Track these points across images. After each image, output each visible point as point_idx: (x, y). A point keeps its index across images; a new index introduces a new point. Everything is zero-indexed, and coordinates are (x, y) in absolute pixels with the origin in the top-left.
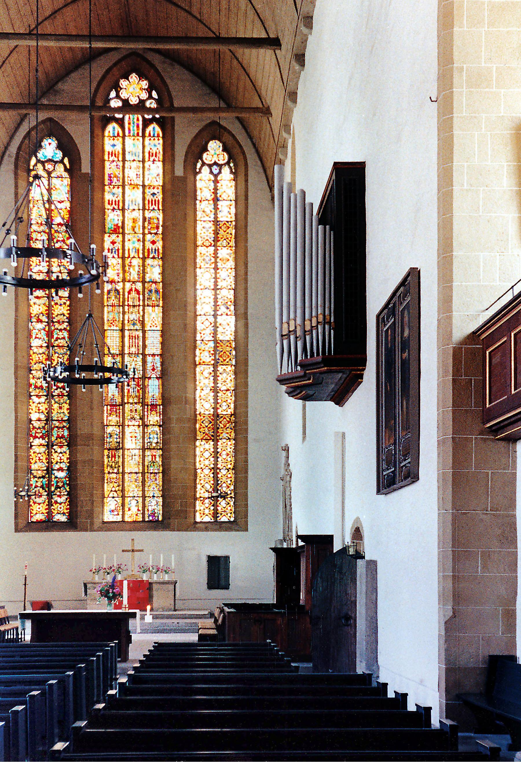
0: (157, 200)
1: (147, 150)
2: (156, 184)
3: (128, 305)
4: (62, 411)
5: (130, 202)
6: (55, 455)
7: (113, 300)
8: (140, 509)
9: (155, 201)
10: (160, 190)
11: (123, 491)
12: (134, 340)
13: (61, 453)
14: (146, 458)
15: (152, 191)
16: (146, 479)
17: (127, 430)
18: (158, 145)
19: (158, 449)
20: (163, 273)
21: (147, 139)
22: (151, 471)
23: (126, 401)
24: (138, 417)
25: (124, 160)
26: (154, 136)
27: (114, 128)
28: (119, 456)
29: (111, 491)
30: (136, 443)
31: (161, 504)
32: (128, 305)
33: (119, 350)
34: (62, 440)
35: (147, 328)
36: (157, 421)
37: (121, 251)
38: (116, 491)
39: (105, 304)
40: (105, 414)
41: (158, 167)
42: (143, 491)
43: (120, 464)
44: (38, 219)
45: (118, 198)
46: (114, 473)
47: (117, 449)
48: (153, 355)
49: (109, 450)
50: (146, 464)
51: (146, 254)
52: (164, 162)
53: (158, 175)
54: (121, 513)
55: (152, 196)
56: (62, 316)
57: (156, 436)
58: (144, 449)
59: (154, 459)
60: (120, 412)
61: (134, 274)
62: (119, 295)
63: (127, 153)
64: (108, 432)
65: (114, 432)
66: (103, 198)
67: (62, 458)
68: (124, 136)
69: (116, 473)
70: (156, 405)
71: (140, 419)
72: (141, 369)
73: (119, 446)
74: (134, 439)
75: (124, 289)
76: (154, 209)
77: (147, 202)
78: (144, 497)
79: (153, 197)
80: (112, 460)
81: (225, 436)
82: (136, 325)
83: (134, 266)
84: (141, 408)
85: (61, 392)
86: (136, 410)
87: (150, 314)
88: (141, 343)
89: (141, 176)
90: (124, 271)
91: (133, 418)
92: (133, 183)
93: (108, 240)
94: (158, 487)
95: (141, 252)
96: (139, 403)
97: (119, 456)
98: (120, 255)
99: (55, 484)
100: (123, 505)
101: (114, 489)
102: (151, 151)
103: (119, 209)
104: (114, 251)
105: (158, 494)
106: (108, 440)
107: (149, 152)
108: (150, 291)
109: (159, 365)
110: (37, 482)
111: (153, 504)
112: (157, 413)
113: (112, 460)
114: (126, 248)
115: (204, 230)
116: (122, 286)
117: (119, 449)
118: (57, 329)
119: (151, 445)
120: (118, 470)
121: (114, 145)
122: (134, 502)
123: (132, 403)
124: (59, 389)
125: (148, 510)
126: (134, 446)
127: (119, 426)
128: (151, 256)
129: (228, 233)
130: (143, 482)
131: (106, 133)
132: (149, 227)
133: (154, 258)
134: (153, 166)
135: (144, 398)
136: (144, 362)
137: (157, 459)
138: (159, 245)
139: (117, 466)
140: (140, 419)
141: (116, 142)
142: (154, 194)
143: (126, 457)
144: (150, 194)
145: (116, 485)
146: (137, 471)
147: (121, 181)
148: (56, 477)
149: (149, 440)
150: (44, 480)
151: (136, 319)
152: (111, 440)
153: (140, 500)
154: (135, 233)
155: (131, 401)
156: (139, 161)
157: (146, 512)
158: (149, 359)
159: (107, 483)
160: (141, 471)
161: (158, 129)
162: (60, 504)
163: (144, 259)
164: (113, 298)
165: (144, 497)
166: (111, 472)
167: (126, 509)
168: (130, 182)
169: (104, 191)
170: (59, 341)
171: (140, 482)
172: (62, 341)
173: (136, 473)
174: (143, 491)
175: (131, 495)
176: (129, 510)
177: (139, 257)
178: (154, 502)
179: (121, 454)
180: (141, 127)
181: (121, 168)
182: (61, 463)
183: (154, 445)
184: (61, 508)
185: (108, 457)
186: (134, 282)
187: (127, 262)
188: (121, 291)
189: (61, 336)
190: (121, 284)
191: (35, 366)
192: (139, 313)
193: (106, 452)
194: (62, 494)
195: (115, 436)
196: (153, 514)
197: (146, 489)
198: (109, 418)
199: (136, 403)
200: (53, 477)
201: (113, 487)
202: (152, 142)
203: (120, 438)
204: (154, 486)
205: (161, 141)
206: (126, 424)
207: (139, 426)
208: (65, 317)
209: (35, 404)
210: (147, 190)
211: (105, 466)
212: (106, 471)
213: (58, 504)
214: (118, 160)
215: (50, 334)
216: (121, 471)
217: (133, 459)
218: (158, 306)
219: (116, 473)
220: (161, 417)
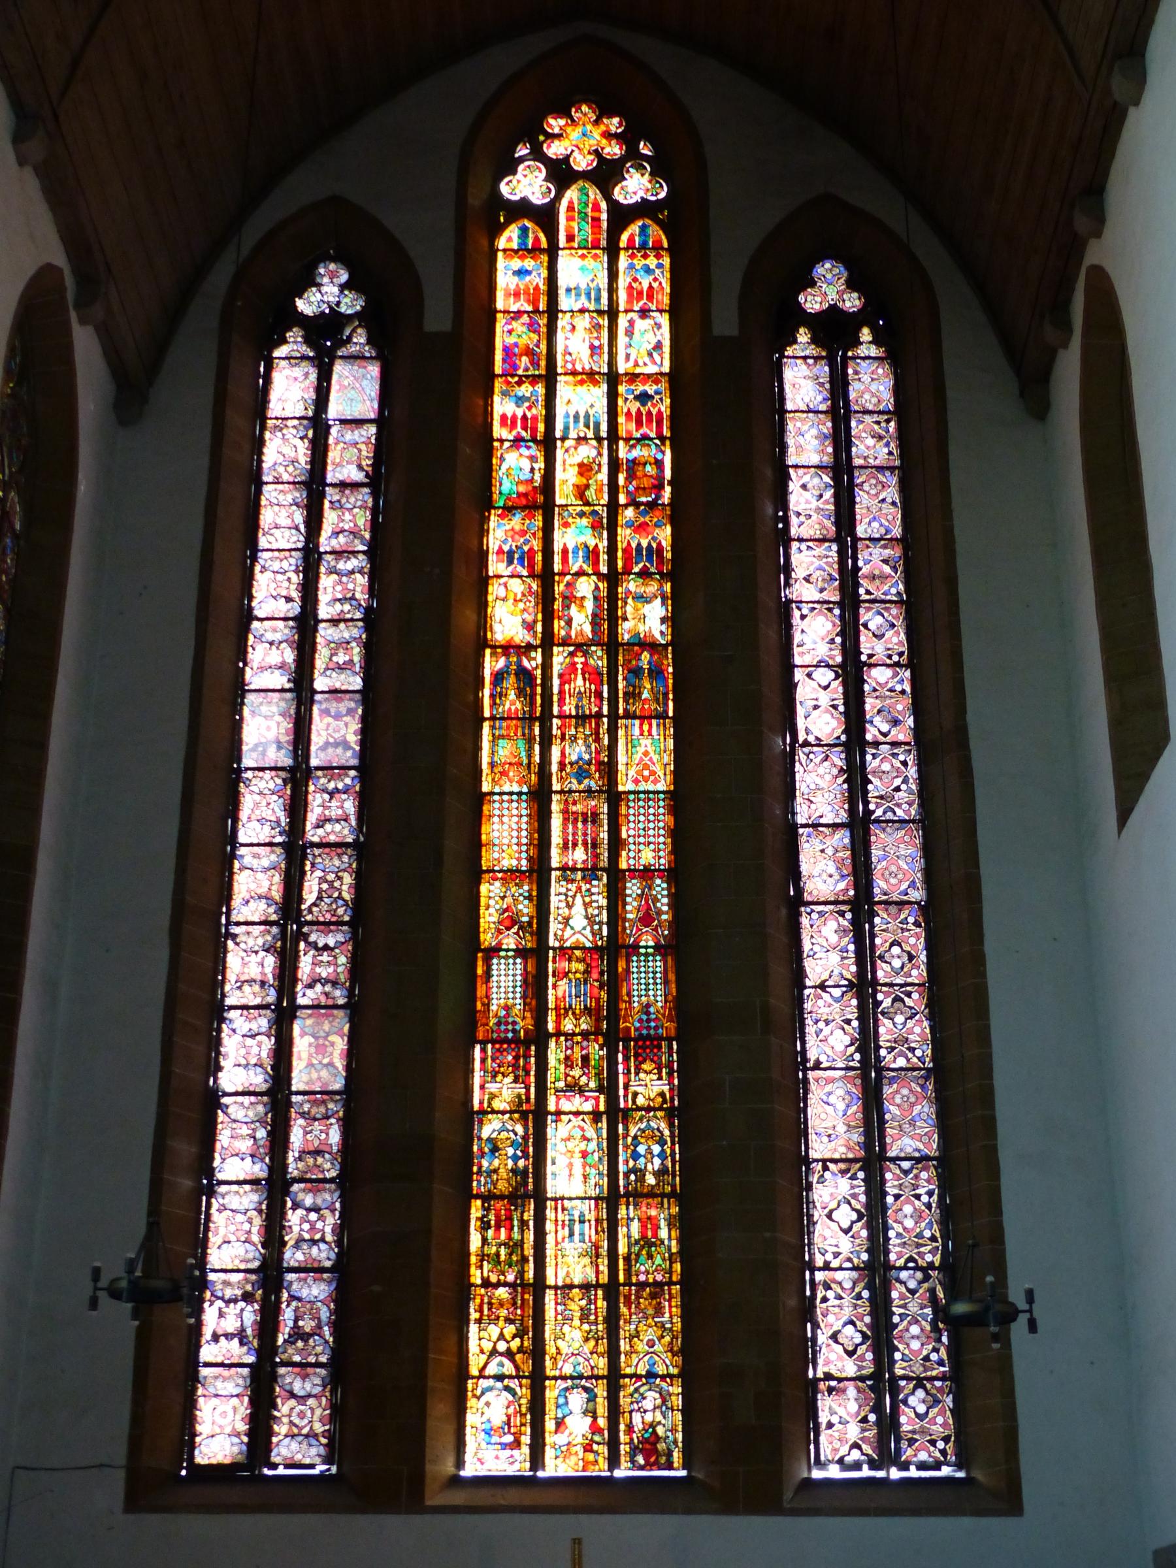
0: (654, 411)
1: (623, 282)
2: (652, 369)
3: (562, 716)
4: (326, 1061)
5: (571, 419)
6: (294, 1218)
7: (512, 702)
8: (602, 1422)
9: (649, 413)
10: (663, 386)
11: (538, 1352)
12: (580, 825)
13: (316, 1209)
14: (622, 1231)
15: (640, 388)
16: (624, 1310)
17: (557, 1134)
18: (658, 271)
19: (663, 1195)
20: (673, 620)
21: (623, 261)
22: (642, 1278)
23: (551, 1027)
24: (592, 1085)
25: (553, 311)
26: (644, 246)
27: (524, 231)
28: (523, 1224)
29: (494, 1352)
30: (585, 1177)
31: (678, 1402)
32: (562, 716)
33: (529, 859)
34: (320, 1160)
35: (625, 785)
36: (662, 1094)
37: (539, 557)
38: (509, 1354)
39: (487, 714)
40: (477, 1081)
41: (659, 326)
42: (613, 1354)
43: (529, 1251)
44: (281, 469)
45: (534, 411)
46: (505, 1284)
47: (515, 1198)
48: (646, 874)
49: (487, 1198)
50: (622, 1249)
51: (620, 564)
52: (675, 312)
53: (658, 346)
54: (526, 1440)
55: (638, 404)
56: (339, 750)
57: (656, 1149)
58: (611, 1199)
59: (650, 1234)
60: (527, 1063)
61: (581, 621)
62: (533, 686)
63: (561, 292)
64: (485, 1135)
65: (504, 1135)
66: (488, 414)
67: (319, 1225)
68: (553, 252)
69: (512, 1285)
70: (661, 1038)
71: (600, 1089)
72: (605, 916)
73: (526, 1184)
74: (578, 1162)
75: (547, 666)
76: (645, 437)
77: (621, 419)
78: (614, 1378)
79: (644, 405)
80: (497, 1237)
81: (909, 1150)
82: (590, 776)
83: (583, 598)
84: (603, 1053)
85: (326, 994)
86: (586, 1059)
87: (631, 744)
88: (604, 835)
89: (606, 349)
90: (548, 617)
91: (574, 1088)
92: (579, 368)
93: (499, 525)
94: (667, 1339)
95: (603, 557)
96: (597, 1032)
97: (523, 1224)
98: (538, 567)
99: (291, 1324)
100: (537, 1407)
101: (502, 1346)
102: (634, 285)
103: (534, 439)
104: (516, 556)
105: (666, 1364)
106: (485, 1163)
107: (630, 287)
108: (637, 672)
109: (663, 904)
110: (221, 1315)
111: (648, 1404)
112: (659, 1068)
113: (497, 1237)
114: (557, 547)
115: (807, 495)
116: (539, 660)
117: (527, 1196)
118: (325, 790)
119: (641, 1178)
120: (521, 1274)
121: (520, 273)
122: (577, 1400)
123: (569, 1036)
124: (318, 987)
125: (630, 1429)
126: (577, 1188)
127: (524, 1116)
128: (636, 569)
129: (883, 500)
130: (613, 1321)
131: (502, 243)
132: (631, 488)
133: (644, 574)
134: (641, 325)
135: (614, 1014)
136: (615, 895)
137: (663, 1233)
138: (665, 535)
139: (514, 1258)
140: (600, 1089)
141: (529, 264)
142: (644, 398)
143: (549, 1226)
144: (631, 397)
145: (510, 1330)
146: (592, 1278)
147: (543, 363)
148: (292, 1298)
149: (631, 1163)
150: (249, 1308)
151: (587, 757)
152: (496, 1163)
153: (601, 1391)
154: (587, 504)
155: (568, 1025)
156: (600, 312)
157: (623, 1438)
158: (633, 888)
159: (479, 1321)
160: (604, 1279)
161: (655, 232)
162: (302, 1399)
163: (613, 578)
164: (512, 695)
165: (614, 1378)
166: (494, 1279)
167: (550, 1425)
168: (569, 366)
169: (490, 393)
170: (328, 827)
171: (600, 1318)
172: (338, 827)
173: (586, 1287)
174: (613, 1354)
175: (568, 1370)
176: (560, 1424)
177: (597, 573)
178: (651, 1399)
179: (529, 1215)
180: (605, 225)
181: (544, 330)
182: (314, 1242)
183: (651, 1180)
184: (302, 1415)
185: (485, 1226)
186: (579, 646)
187: (559, 588)
188: (539, 672)
189: (335, 812)
190: (538, 655)
191: (244, 909)
192: (597, 740)
193: (476, 1210)
194: (312, 1359)
195: (510, 1151)
196: (649, 1446)
197: (624, 1346)
198: (492, 1087)
199: (585, 1035)
200: (285, 1295)
201: (501, 1336)
202: (639, 263)
203: (525, 1155)
204: (650, 1334)
205: (666, 261)
206: (552, 1107)
207: (596, 1116)
208: (349, 753)
209: (237, 1038)
210: (621, 389)
211: (473, 1259)
212: (476, 1277)
213: (293, 1402)
214: (536, 311)
215: (297, 808)
216: (530, 1275)
217: (577, 1237)
218: (662, 716)
219: (512, 1285)
220: (676, 1082)
